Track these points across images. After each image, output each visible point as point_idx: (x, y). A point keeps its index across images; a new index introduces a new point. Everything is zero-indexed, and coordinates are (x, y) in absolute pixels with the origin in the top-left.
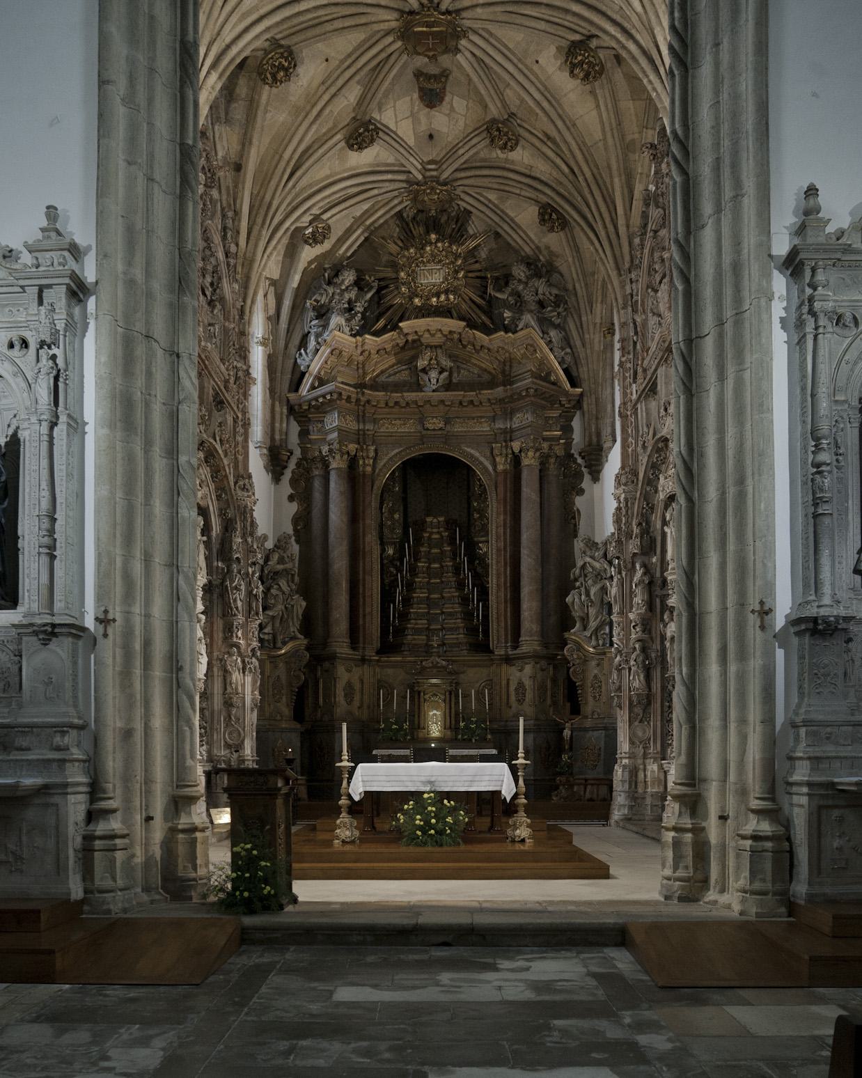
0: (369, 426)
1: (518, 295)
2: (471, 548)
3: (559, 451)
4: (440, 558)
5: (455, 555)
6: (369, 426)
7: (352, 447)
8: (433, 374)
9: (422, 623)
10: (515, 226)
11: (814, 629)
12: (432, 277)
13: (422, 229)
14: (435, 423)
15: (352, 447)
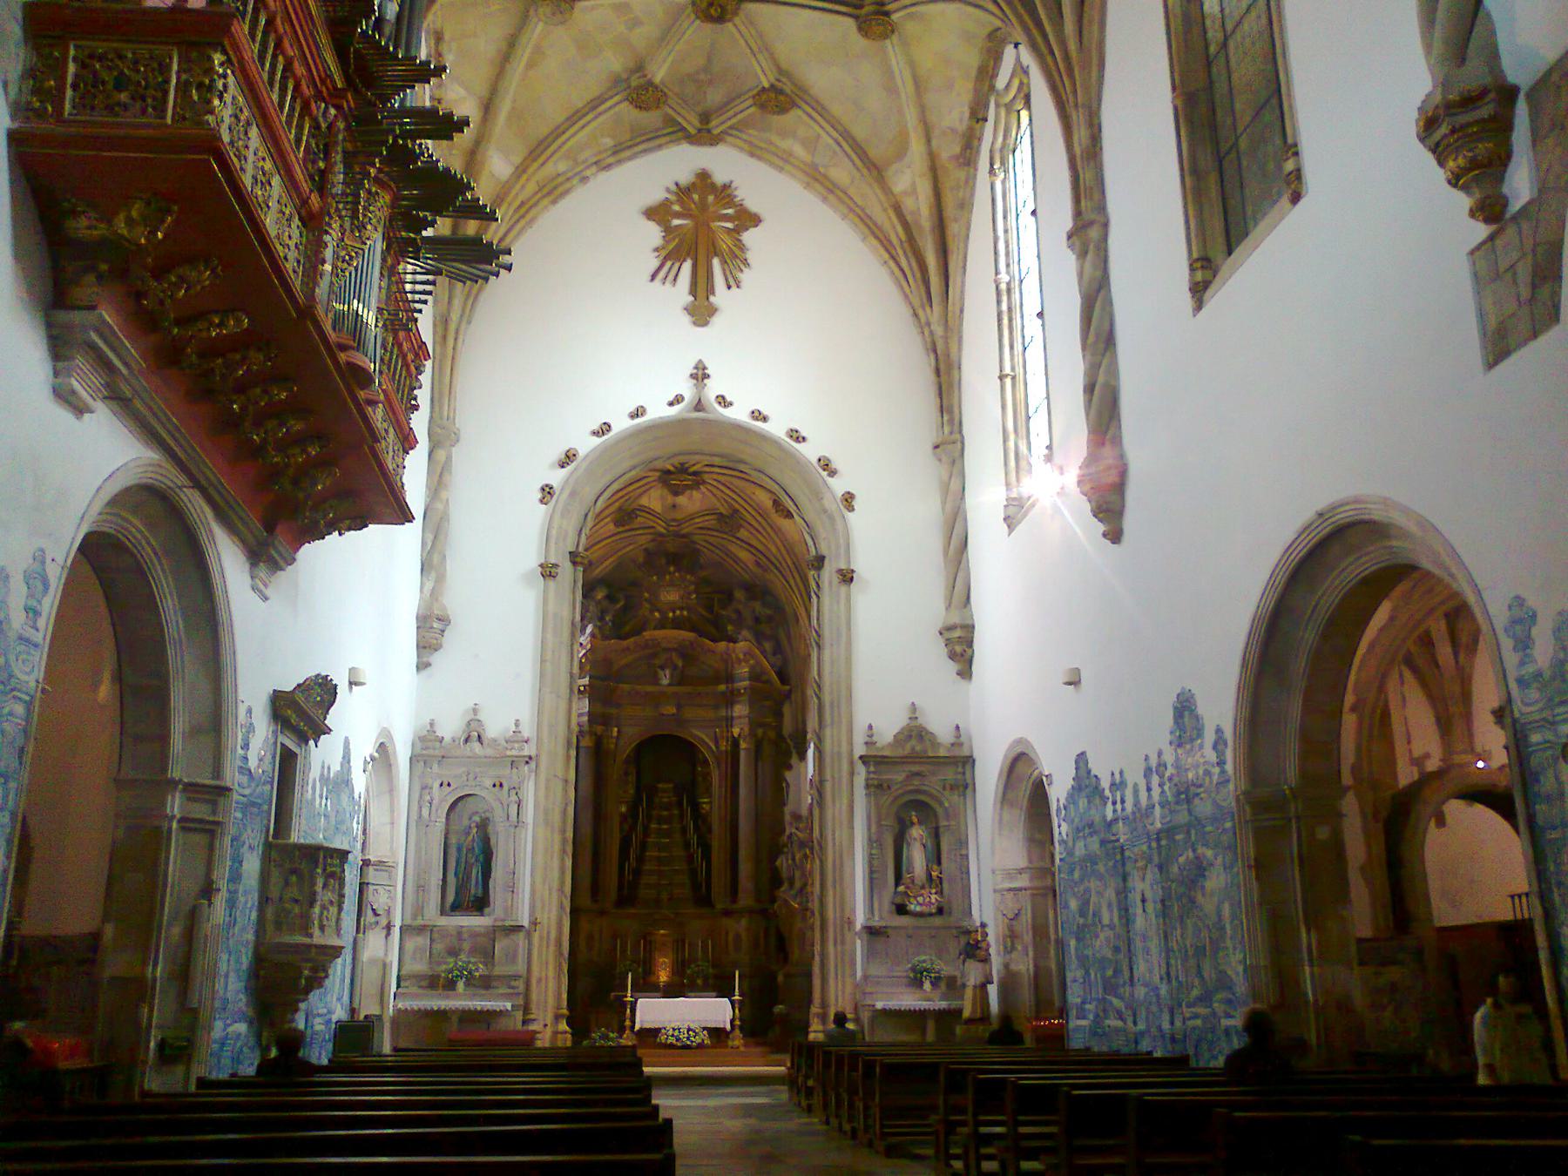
0: (613, 711)
1: (738, 612)
2: (695, 807)
3: (772, 734)
4: (668, 820)
5: (682, 817)
6: (613, 711)
7: (599, 729)
8: (667, 672)
9: (653, 879)
10: (737, 560)
11: (871, 931)
12: (670, 596)
13: (663, 561)
14: (671, 710)
15: (599, 729)
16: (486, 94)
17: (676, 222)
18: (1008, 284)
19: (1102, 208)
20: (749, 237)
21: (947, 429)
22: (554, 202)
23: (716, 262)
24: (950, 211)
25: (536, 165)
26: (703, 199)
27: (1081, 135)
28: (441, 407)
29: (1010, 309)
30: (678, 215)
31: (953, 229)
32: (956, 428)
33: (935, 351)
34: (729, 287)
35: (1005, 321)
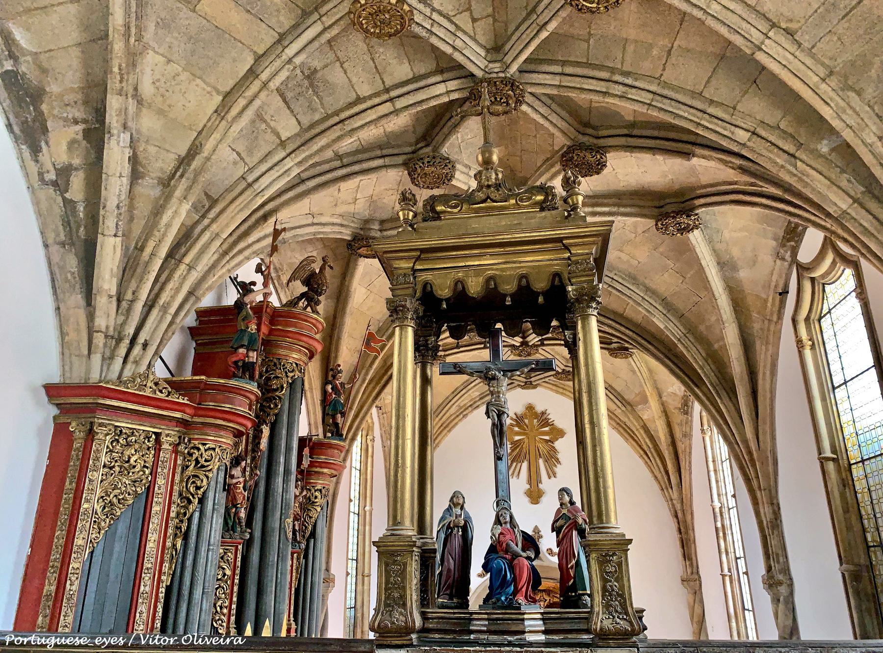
17: (517, 438)
18: (721, 508)
19: (786, 570)
20: (558, 444)
21: (689, 571)
22: (449, 431)
23: (541, 461)
24: (678, 435)
25: (437, 419)
26: (531, 422)
27: (766, 511)
29: (723, 526)
30: (518, 434)
31: (681, 447)
32: (695, 570)
33: (677, 517)
34: (550, 478)
35: (721, 534)
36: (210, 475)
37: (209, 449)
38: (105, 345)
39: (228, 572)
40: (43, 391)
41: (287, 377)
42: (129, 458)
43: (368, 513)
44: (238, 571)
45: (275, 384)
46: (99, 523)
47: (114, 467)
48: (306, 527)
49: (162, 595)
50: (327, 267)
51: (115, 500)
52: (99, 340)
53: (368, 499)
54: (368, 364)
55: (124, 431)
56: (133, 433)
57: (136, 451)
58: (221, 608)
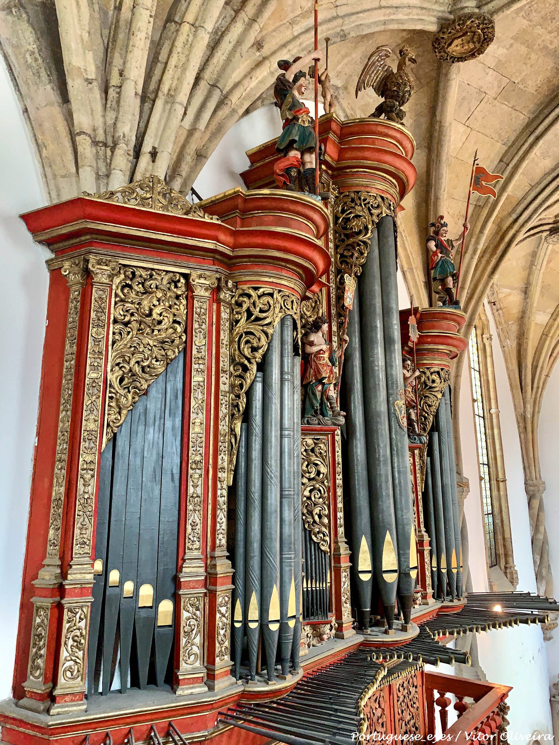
16: (522, 285)
28: (530, 472)
36: (270, 331)
37: (264, 294)
38: (97, 157)
39: (323, 469)
40: (22, 226)
41: (372, 214)
42: (151, 310)
43: (494, 416)
44: (339, 469)
45: (356, 225)
46: (117, 400)
47: (129, 322)
48: (426, 418)
49: (222, 500)
50: (408, 63)
51: (137, 369)
52: (85, 146)
53: (493, 402)
54: (477, 230)
55: (137, 273)
56: (151, 276)
57: (159, 300)
58: (320, 516)
